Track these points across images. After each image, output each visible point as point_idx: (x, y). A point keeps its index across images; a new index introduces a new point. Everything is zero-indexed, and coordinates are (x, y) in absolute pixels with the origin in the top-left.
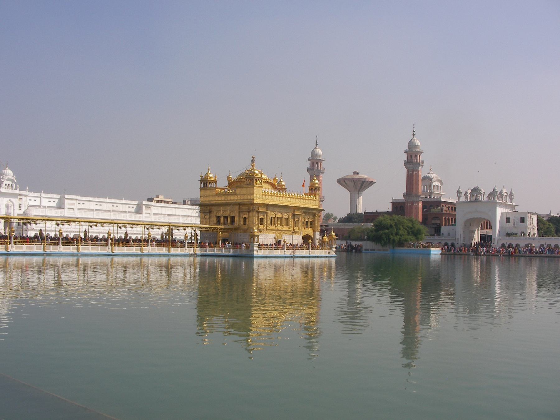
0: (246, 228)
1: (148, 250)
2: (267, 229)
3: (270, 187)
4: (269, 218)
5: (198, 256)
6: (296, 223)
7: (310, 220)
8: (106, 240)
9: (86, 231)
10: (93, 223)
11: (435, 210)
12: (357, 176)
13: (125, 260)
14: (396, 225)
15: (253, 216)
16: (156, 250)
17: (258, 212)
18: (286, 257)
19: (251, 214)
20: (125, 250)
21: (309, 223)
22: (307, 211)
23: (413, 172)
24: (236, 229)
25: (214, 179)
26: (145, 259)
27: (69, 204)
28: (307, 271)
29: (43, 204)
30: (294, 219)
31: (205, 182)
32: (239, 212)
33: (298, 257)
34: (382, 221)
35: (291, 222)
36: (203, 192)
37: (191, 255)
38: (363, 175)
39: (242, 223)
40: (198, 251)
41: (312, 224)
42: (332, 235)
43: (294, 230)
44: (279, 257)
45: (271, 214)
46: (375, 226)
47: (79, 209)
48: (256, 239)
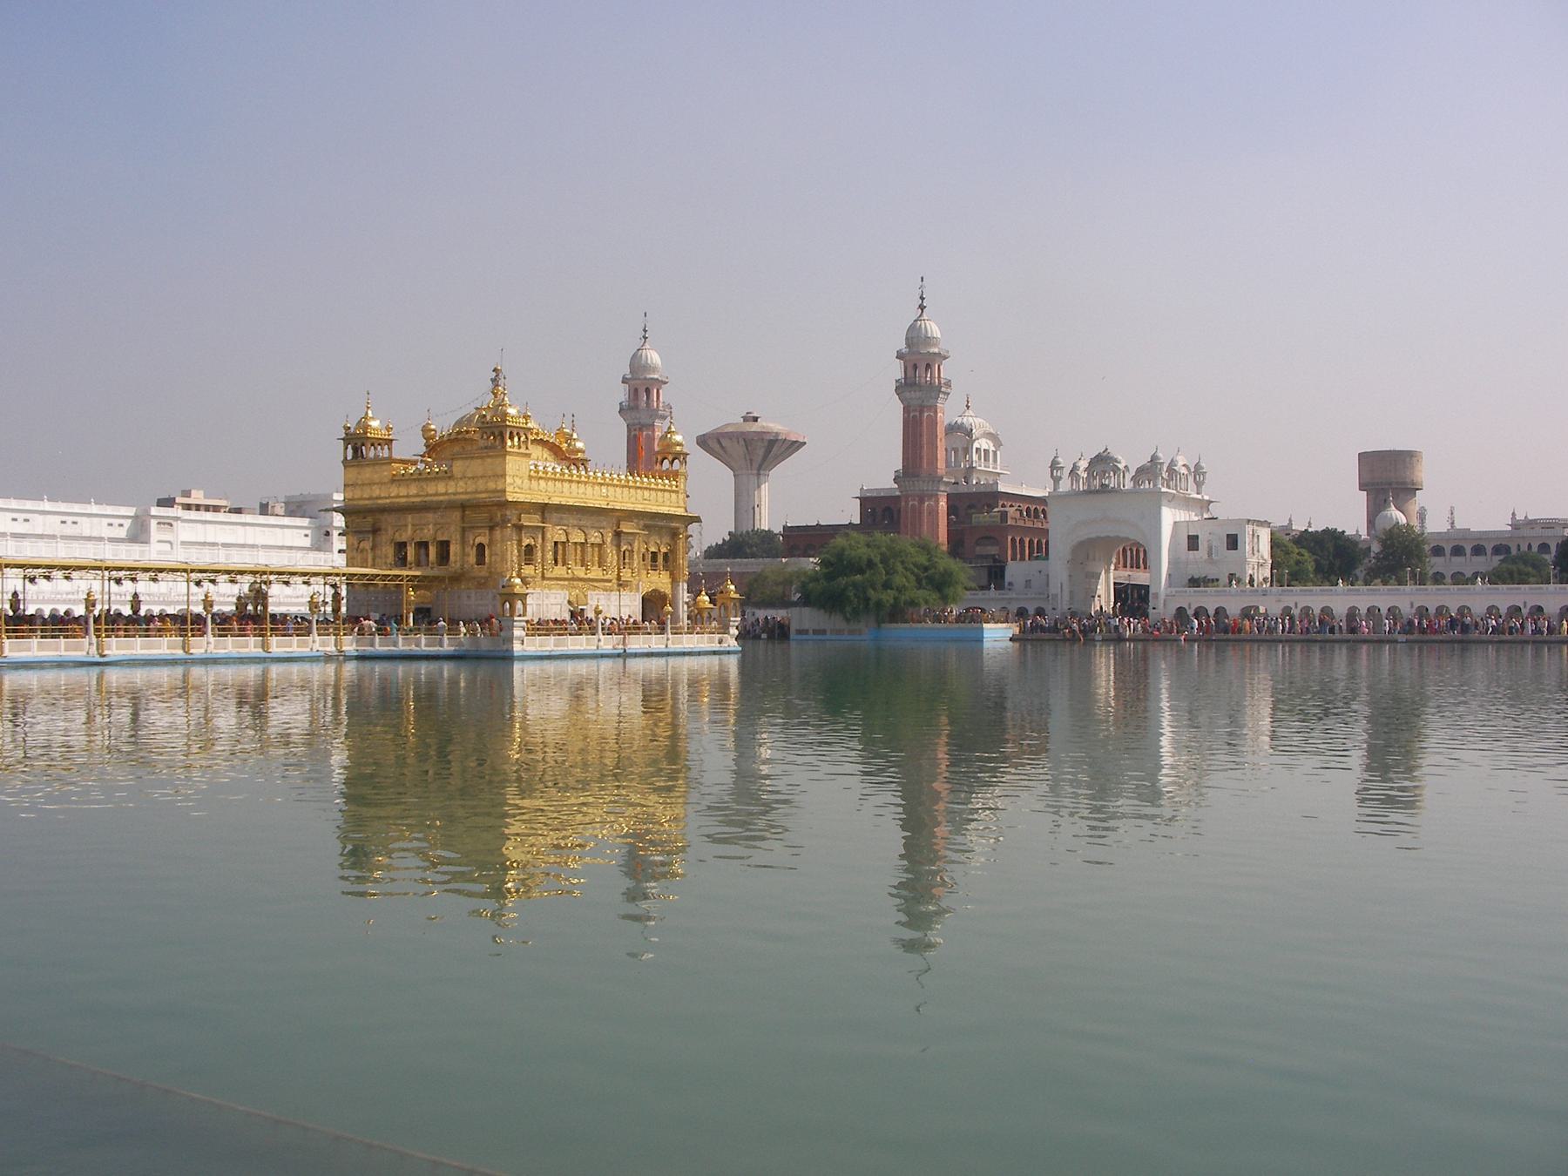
0: (484, 573)
1: (207, 644)
2: (543, 578)
3: (547, 454)
4: (550, 546)
5: (348, 658)
6: (624, 558)
7: (664, 550)
9: (15, 594)
10: (36, 571)
11: (982, 518)
12: (755, 427)
13: (139, 676)
14: (884, 561)
16: (230, 646)
17: (519, 528)
18: (603, 656)
19: (498, 533)
20: (138, 647)
21: (660, 559)
22: (655, 522)
23: (921, 412)
24: (456, 578)
25: (383, 434)
26: (197, 672)
28: (655, 696)
30: (619, 546)
31: (357, 443)
32: (464, 530)
33: (636, 655)
34: (843, 549)
35: (611, 556)
36: (353, 472)
37: (328, 658)
39: (472, 559)
40: (350, 645)
41: (668, 561)
42: (729, 592)
43: (619, 578)
44: (588, 657)
45: (556, 533)
46: (824, 563)
48: (519, 605)
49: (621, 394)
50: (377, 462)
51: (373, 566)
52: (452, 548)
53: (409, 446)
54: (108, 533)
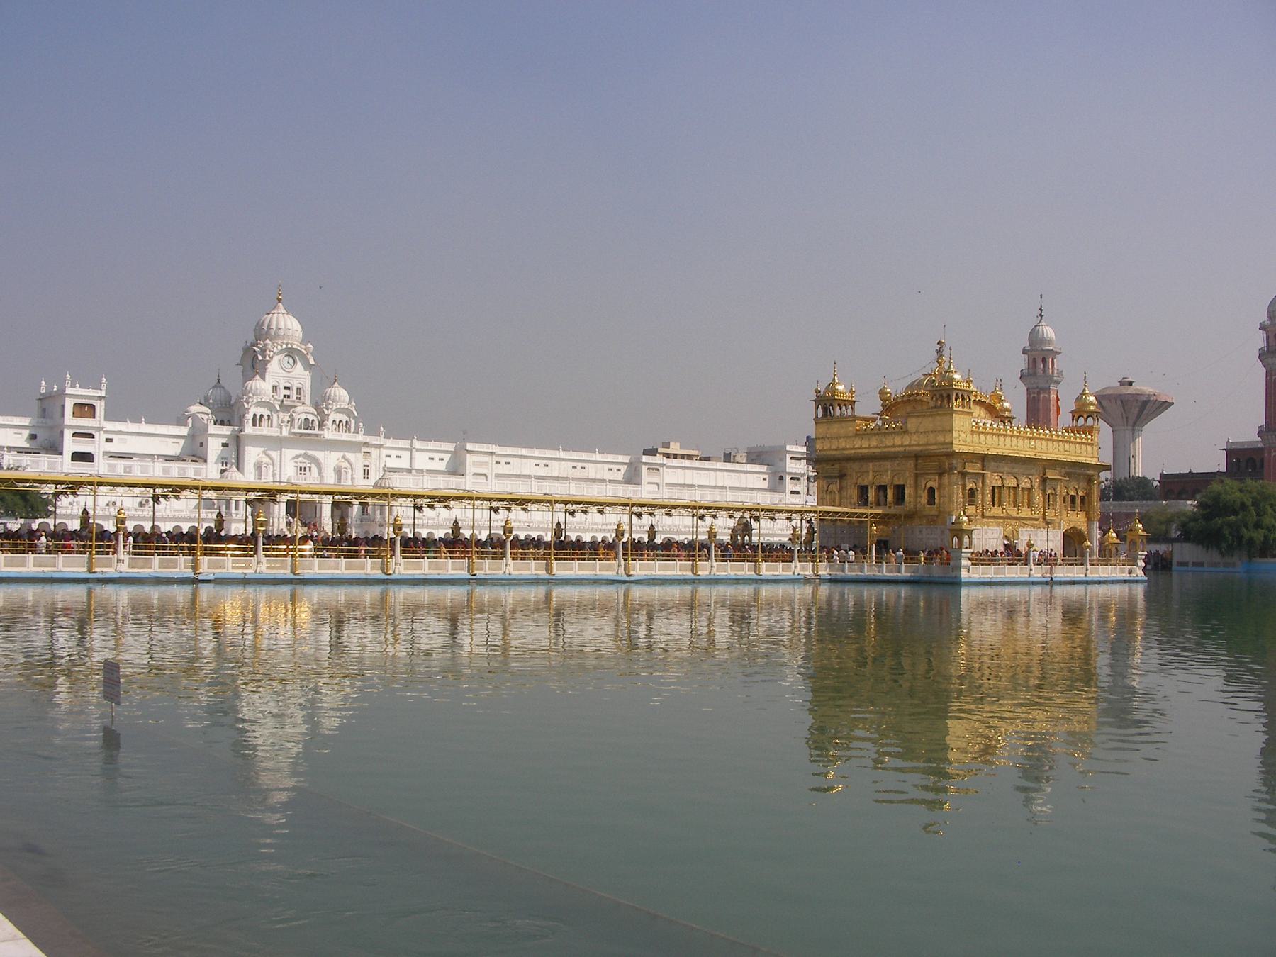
0: (934, 512)
1: (711, 568)
2: (983, 516)
3: (983, 413)
4: (988, 490)
5: (823, 581)
6: (1048, 500)
7: (1081, 494)
8: (610, 546)
9: (559, 524)
12: (1130, 390)
13: (656, 592)
14: (1255, 504)
15: (950, 484)
16: (729, 569)
17: (963, 474)
18: (1034, 583)
19: (946, 479)
20: (658, 569)
21: (1078, 501)
24: (910, 516)
25: (847, 396)
26: (703, 591)
27: (475, 464)
28: (1073, 615)
29: (417, 465)
30: (1044, 490)
31: (826, 404)
32: (916, 476)
33: (1060, 583)
34: (1219, 494)
35: (1038, 498)
36: (823, 429)
37: (807, 581)
38: (1144, 387)
39: (924, 500)
40: (824, 570)
41: (1084, 503)
42: (1137, 530)
43: (1044, 517)
44: (1025, 582)
45: (993, 479)
47: (497, 475)
48: (966, 540)
49: (1021, 363)
50: (843, 419)
51: (840, 505)
52: (907, 491)
53: (869, 406)
54: (608, 476)
